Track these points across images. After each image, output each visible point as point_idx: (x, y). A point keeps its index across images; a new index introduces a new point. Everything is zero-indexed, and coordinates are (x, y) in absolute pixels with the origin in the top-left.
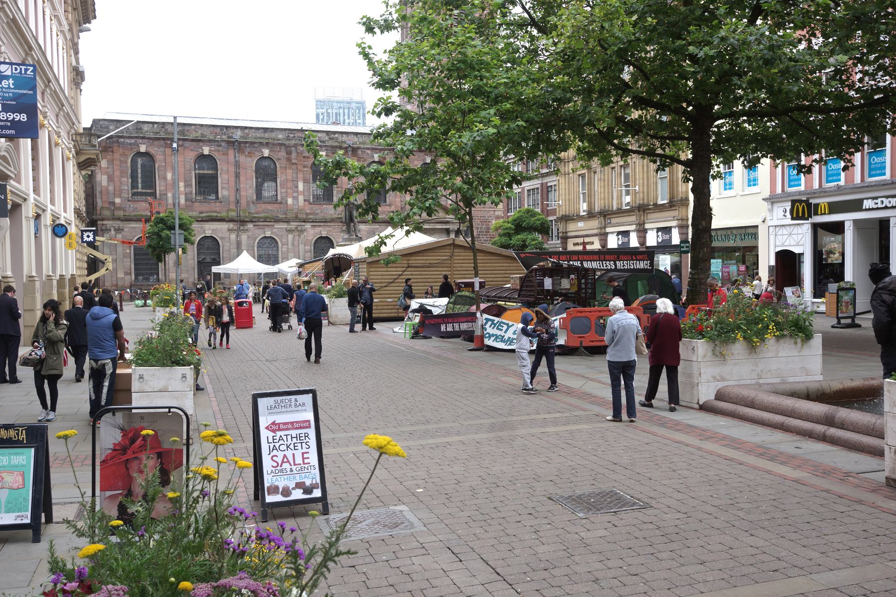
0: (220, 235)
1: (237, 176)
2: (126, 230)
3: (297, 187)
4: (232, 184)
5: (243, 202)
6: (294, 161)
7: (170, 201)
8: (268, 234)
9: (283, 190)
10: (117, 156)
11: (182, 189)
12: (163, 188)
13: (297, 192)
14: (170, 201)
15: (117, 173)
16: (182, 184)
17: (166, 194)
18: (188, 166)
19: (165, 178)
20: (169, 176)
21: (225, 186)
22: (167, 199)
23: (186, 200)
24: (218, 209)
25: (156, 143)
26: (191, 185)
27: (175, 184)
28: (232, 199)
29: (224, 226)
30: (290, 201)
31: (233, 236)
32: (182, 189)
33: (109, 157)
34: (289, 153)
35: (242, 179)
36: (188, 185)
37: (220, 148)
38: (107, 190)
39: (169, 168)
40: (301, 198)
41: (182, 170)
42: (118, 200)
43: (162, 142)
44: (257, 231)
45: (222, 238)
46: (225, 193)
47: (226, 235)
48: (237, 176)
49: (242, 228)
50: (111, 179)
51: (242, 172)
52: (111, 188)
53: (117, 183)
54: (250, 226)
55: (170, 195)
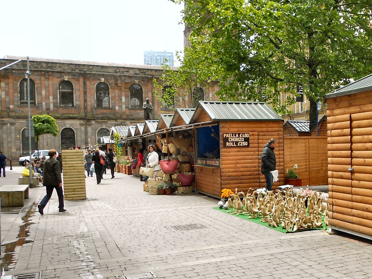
0: (75, 127)
1: (85, 93)
2: (17, 124)
3: (121, 100)
4: (82, 98)
5: (89, 108)
6: (119, 85)
7: (44, 107)
8: (104, 127)
9: (113, 102)
10: (11, 81)
11: (51, 100)
12: (40, 100)
13: (122, 102)
14: (44, 107)
15: (11, 91)
16: (51, 98)
17: (42, 103)
18: (55, 87)
19: (41, 94)
20: (44, 93)
21: (78, 99)
22: (42, 106)
23: (54, 107)
24: (73, 112)
25: (36, 73)
26: (57, 98)
27: (47, 97)
28: (82, 106)
29: (77, 122)
30: (117, 108)
31: (83, 128)
32: (51, 100)
33: (6, 81)
34: (116, 80)
35: (88, 95)
36: (55, 98)
37: (75, 77)
38: (5, 101)
39: (43, 88)
40: (124, 106)
41: (51, 89)
42: (11, 107)
43: (39, 73)
44: (97, 125)
45: (76, 129)
46: (78, 103)
47: (79, 127)
48: (85, 93)
49: (88, 123)
50: (7, 94)
51: (88, 91)
52: (7, 99)
53: (11, 97)
54: (93, 122)
55: (44, 104)
